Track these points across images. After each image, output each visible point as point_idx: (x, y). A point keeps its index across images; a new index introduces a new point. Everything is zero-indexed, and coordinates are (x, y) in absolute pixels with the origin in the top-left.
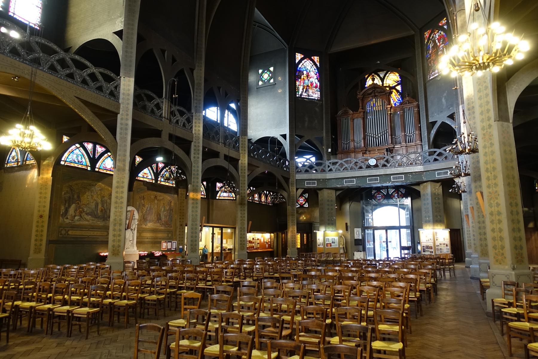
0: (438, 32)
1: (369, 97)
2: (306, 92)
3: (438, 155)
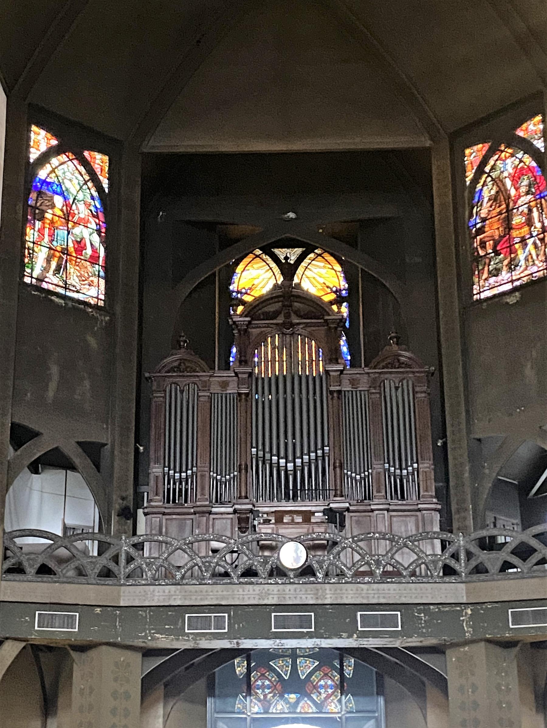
0: (512, 155)
2: (58, 270)
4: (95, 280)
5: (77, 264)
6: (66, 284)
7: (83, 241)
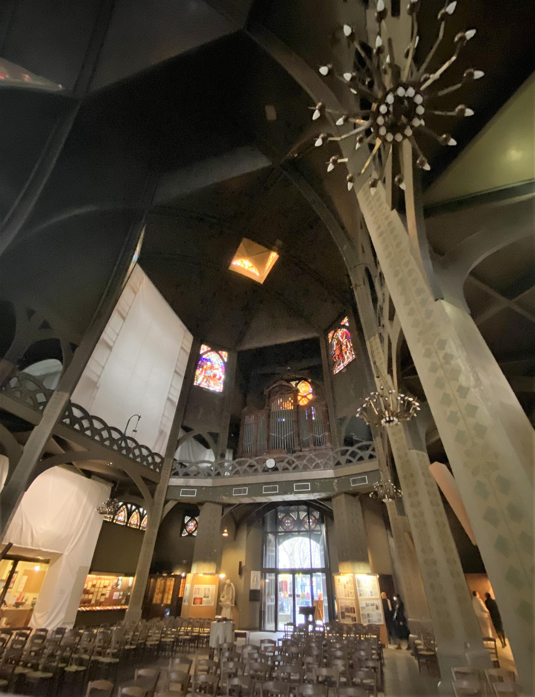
1: (276, 395)
2: (206, 382)
3: (350, 455)
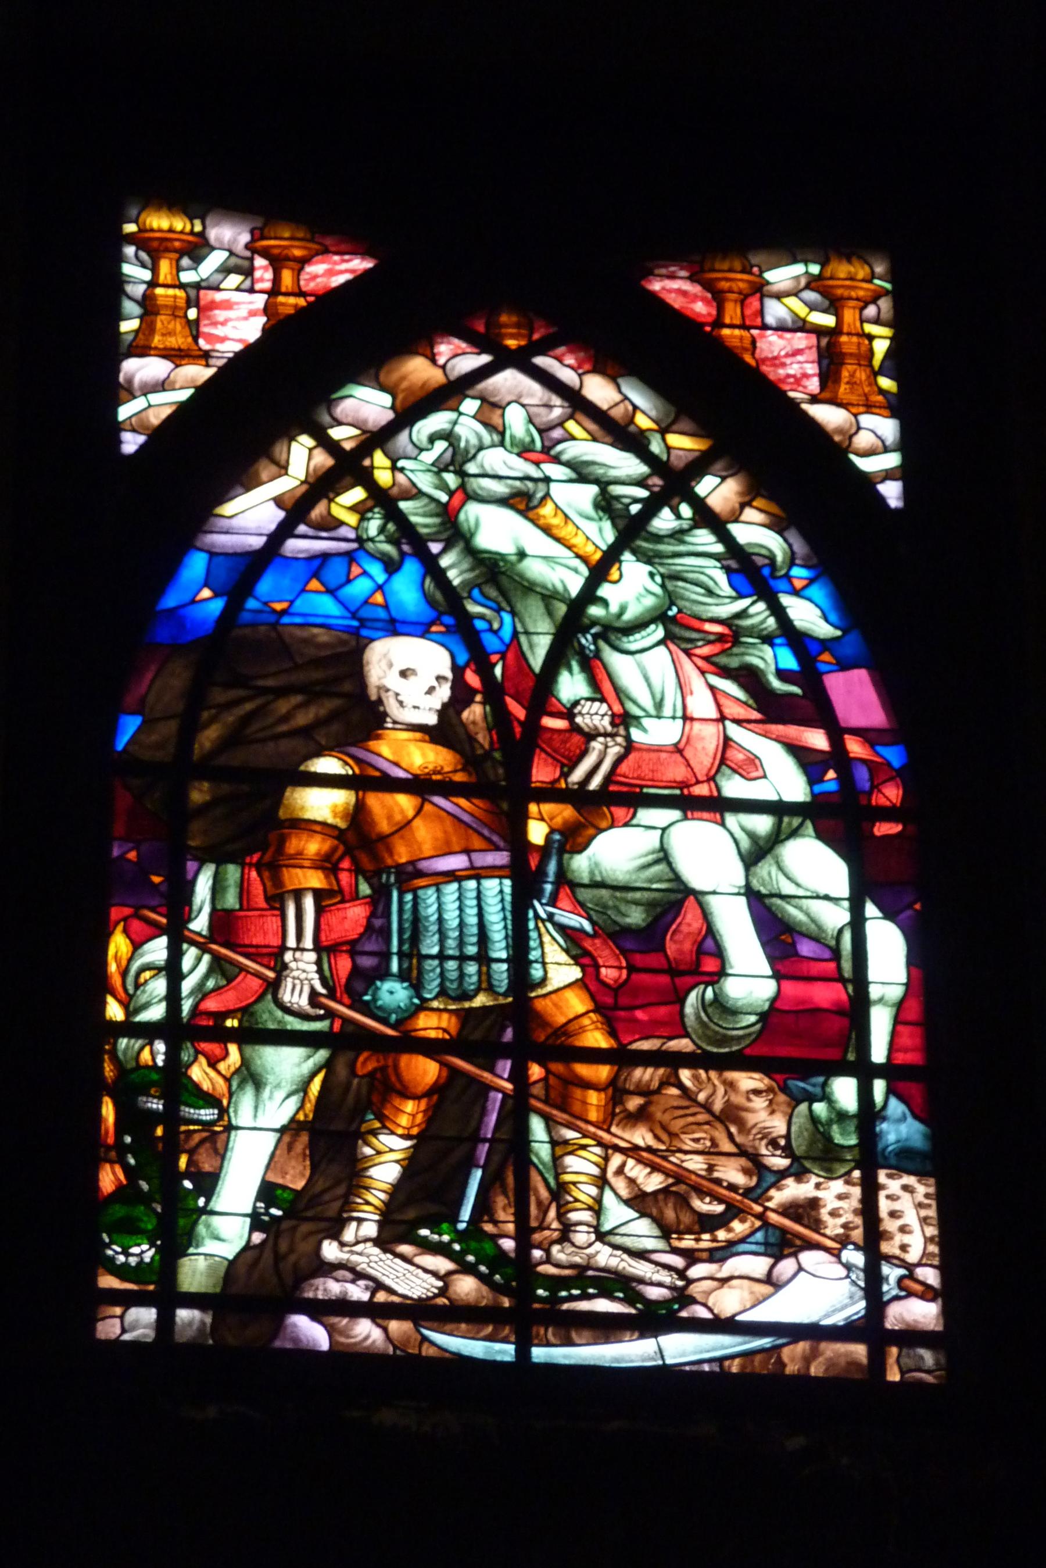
4: (836, 1196)
5: (634, 1103)
6: (515, 1275)
7: (690, 920)
